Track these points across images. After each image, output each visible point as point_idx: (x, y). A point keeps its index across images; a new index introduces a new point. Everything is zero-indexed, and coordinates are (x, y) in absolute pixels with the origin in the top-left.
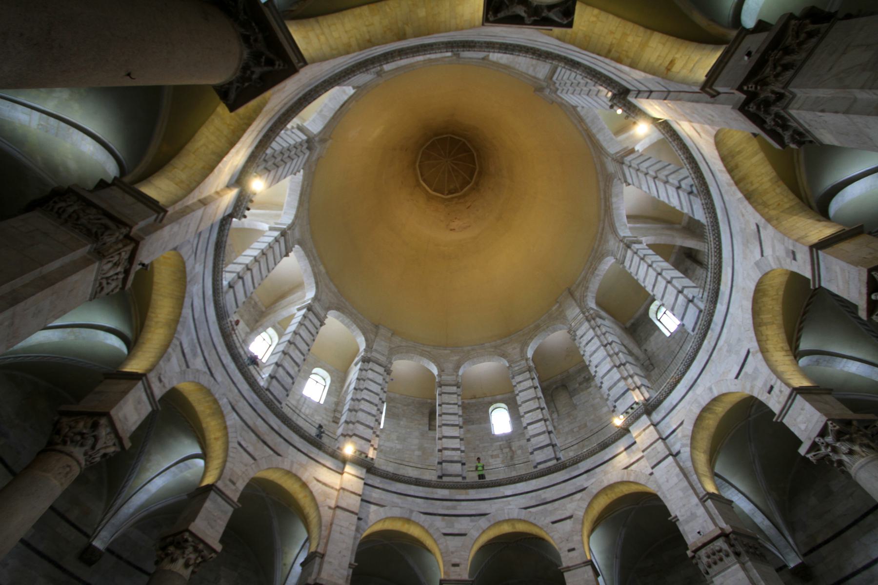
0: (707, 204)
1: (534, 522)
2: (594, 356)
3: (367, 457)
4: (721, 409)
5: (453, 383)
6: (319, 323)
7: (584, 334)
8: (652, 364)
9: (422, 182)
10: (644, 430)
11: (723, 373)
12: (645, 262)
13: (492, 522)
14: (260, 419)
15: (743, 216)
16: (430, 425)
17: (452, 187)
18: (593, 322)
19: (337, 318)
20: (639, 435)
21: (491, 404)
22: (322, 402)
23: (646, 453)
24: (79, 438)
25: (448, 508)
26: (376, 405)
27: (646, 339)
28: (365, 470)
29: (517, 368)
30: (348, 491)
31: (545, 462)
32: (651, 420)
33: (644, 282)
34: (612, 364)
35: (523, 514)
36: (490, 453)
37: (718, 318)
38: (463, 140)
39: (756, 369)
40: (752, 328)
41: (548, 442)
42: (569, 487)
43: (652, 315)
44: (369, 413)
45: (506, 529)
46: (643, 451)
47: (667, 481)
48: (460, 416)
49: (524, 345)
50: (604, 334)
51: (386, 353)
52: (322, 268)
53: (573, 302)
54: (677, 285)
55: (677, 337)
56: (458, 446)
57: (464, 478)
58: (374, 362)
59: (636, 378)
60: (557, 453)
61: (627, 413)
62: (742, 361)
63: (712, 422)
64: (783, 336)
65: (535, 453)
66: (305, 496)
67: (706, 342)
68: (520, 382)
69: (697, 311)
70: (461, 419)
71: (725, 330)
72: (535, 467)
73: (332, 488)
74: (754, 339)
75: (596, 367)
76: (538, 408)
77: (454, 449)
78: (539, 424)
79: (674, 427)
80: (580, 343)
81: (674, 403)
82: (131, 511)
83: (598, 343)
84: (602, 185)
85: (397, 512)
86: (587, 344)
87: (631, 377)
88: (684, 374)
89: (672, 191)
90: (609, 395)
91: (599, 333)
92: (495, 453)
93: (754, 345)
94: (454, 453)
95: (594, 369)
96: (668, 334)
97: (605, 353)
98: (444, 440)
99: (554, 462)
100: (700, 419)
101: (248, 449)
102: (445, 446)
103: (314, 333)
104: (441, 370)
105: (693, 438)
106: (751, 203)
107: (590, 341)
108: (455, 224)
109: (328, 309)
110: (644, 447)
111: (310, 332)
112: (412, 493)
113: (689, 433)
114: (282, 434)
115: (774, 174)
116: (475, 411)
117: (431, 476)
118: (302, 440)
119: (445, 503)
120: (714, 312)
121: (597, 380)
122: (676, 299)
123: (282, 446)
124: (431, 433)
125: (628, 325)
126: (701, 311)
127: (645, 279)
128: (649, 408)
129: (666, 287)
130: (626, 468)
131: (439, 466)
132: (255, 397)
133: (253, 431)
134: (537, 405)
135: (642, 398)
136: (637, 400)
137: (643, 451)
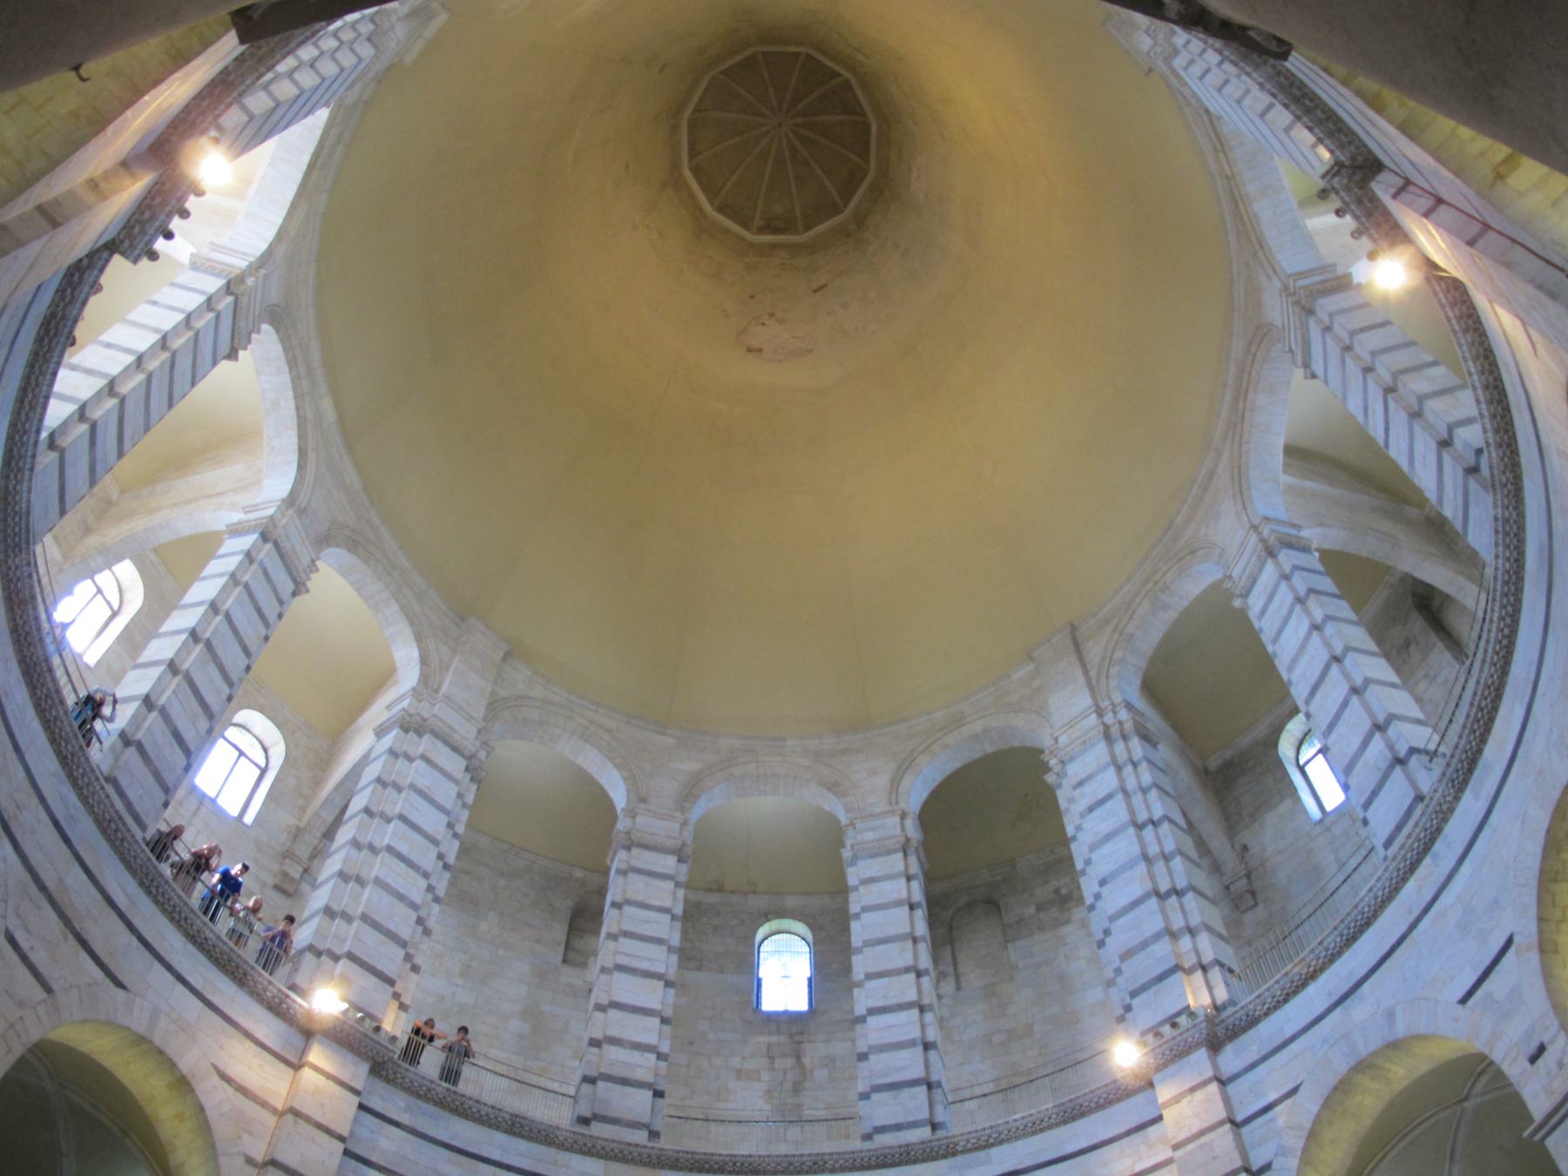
0: (1506, 521)
2: (1106, 849)
3: (378, 1029)
4: (1401, 1071)
5: (669, 843)
6: (291, 587)
7: (1089, 778)
8: (1253, 894)
9: (688, 174)
10: (1192, 1090)
12: (1307, 612)
14: (77, 870)
16: (568, 947)
17: (779, 209)
18: (1119, 747)
19: (345, 573)
20: (1176, 1100)
21: (766, 917)
22: (248, 819)
23: (1178, 1154)
26: (426, 875)
27: (1254, 816)
28: (364, 1068)
29: (869, 836)
30: (308, 1120)
31: (898, 1127)
32: (1215, 1066)
33: (1290, 669)
34: (1148, 886)
36: (736, 1062)
38: (846, 74)
40: (1534, 883)
41: (918, 1072)
43: (1285, 748)
44: (402, 898)
46: (1175, 1147)
48: (670, 949)
49: (905, 766)
50: (1144, 791)
51: (479, 712)
52: (327, 405)
53: (1079, 671)
54: (1375, 707)
55: (1337, 831)
56: (651, 1039)
57: (654, 1135)
58: (436, 735)
59: (1204, 940)
60: (939, 1109)
61: (1157, 1034)
62: (1488, 962)
63: (1371, 1101)
65: (875, 1096)
66: (180, 1117)
67: (1411, 885)
69: (1411, 795)
70: (674, 958)
71: (1467, 865)
72: (867, 1137)
73: (264, 1104)
74: (1533, 911)
75: (1103, 882)
76: (907, 970)
77: (637, 1046)
78: (903, 1016)
79: (1272, 1096)
80: (1071, 800)
81: (1289, 1033)
83: (1124, 816)
86: (1091, 809)
87: (1192, 932)
88: (1332, 958)
89: (1425, 447)
90: (1118, 971)
91: (1131, 783)
92: (750, 1065)
93: (1527, 930)
94: (636, 1057)
95: (1096, 889)
96: (1315, 813)
97: (1136, 849)
98: (612, 1013)
99: (924, 1133)
100: (1342, 1088)
101: (33, 957)
102: (614, 1032)
103: (271, 616)
104: (640, 798)
105: (1312, 1136)
107: (1101, 802)
109: (323, 541)
110: (1182, 1135)
111: (259, 611)
112: (495, 1155)
113: (1307, 1122)
114: (137, 922)
116: (716, 931)
117: (558, 1114)
118: (190, 947)
120: (1451, 810)
121: (1097, 922)
122: (1365, 744)
123: (133, 963)
124: (569, 975)
125: (1214, 763)
126: (1419, 798)
127: (1294, 661)
128: (1220, 1032)
129: (1345, 704)
131: (586, 1088)
132: (73, 798)
133: (53, 902)
134: (907, 960)
135: (1206, 1000)
136: (1191, 1002)
137: (1175, 1147)
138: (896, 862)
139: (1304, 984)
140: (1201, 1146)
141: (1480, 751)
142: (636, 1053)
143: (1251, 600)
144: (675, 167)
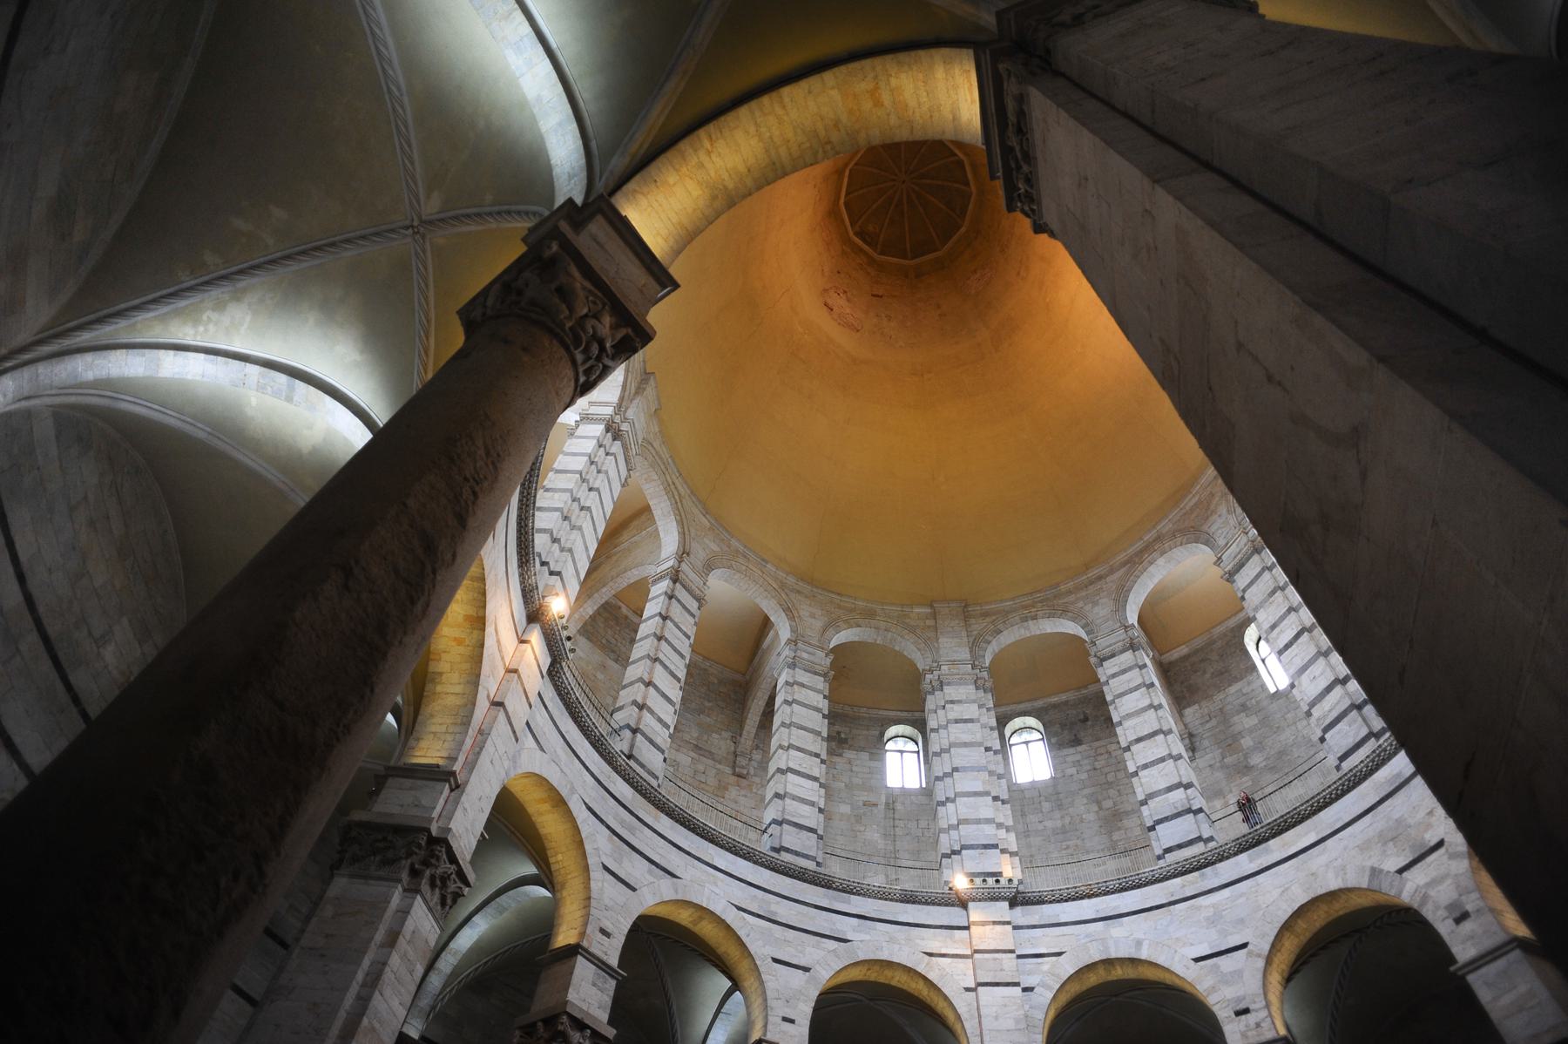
1: (744, 939)
7: (959, 702)
10: (994, 923)
13: (679, 897)
17: (871, 228)
20: (984, 924)
24: (595, 349)
25: (622, 823)
31: (797, 854)
35: (732, 917)
39: (1239, 973)
42: (822, 922)
45: (684, 917)
47: (996, 1018)
49: (832, 624)
53: (964, 633)
64: (1293, 957)
66: (459, 642)
68: (803, 685)
71: (1226, 892)
72: (777, 850)
75: (955, 769)
77: (660, 720)
82: (90, 376)
85: (555, 778)
86: (957, 721)
104: (683, 554)
108: (839, 302)
122: (1170, 789)
127: (1129, 716)
128: (1020, 898)
129: (1162, 760)
130: (931, 955)
138: (820, 683)
141: (1267, 840)
144: (846, 165)
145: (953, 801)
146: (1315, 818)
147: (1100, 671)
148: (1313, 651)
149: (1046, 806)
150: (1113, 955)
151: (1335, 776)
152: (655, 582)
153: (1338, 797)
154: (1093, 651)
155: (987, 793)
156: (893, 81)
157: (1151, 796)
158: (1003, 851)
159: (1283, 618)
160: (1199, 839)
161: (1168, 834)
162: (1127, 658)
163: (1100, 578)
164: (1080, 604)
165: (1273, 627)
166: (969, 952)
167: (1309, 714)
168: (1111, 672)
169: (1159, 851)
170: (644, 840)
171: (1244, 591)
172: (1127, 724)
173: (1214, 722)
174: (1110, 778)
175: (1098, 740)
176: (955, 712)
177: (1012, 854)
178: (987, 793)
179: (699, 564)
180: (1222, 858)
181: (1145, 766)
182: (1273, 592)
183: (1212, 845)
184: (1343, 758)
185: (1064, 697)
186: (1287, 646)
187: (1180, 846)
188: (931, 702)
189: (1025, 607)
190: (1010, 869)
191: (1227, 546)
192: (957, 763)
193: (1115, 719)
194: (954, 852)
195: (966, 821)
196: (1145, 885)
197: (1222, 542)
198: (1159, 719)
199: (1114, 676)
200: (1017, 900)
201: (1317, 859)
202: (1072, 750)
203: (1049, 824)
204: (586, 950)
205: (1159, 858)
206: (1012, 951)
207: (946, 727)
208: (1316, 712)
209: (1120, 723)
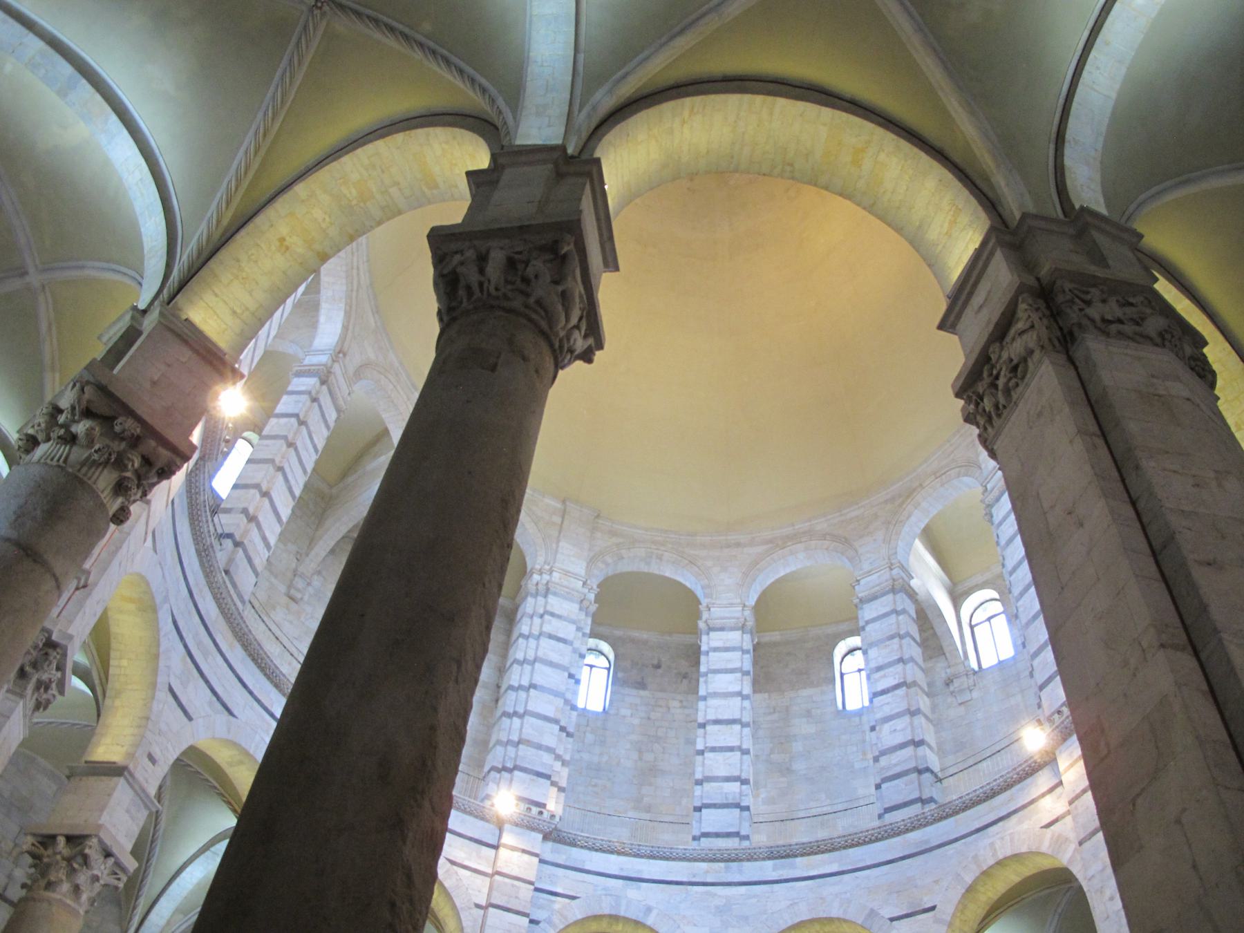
7: (559, 617)
10: (524, 851)
11: (684, 917)
15: (936, 882)
20: (514, 849)
25: (199, 644)
37: (751, 870)
67: (704, 865)
71: (743, 889)
75: (533, 686)
77: (264, 539)
81: (587, 868)
84: (821, 525)
86: (551, 637)
88: (637, 856)
104: (340, 352)
106: (963, 896)
115: (996, 898)
119: (202, 628)
120: (756, 860)
127: (715, 695)
128: (554, 834)
129: (731, 749)
139: (612, 852)
140: (513, 886)
141: (796, 856)
142: (262, 545)
143: (712, 634)
145: (521, 716)
146: (844, 852)
147: (704, 638)
148: (903, 706)
149: (590, 737)
150: (622, 914)
151: (877, 823)
152: (299, 374)
153: (871, 841)
154: (705, 615)
155: (556, 721)
156: (882, 156)
157: (709, 779)
158: (554, 784)
159: (890, 665)
160: (737, 834)
161: (713, 820)
162: (734, 637)
163: (738, 545)
164: (709, 563)
165: (879, 669)
166: (490, 871)
167: (876, 759)
168: (714, 644)
169: (696, 833)
170: (213, 667)
171: (868, 622)
172: (712, 702)
173: (775, 716)
174: (660, 734)
175: (661, 691)
176: (551, 626)
177: (561, 789)
178: (556, 721)
179: (351, 370)
180: (751, 859)
181: (713, 749)
182: (891, 637)
183: (746, 844)
184: (888, 810)
185: (645, 636)
186: (883, 692)
187: (717, 835)
188: (529, 605)
189: (654, 542)
190: (554, 804)
191: (869, 573)
192: (538, 680)
193: (702, 692)
194: (505, 769)
195: (528, 743)
196: (674, 860)
197: (866, 567)
198: (743, 709)
199: (716, 650)
200: (553, 835)
201: (830, 888)
202: (634, 692)
203: (585, 756)
204: (131, 774)
205: (694, 838)
206: (531, 883)
207: (538, 638)
208: (884, 761)
209: (704, 698)
